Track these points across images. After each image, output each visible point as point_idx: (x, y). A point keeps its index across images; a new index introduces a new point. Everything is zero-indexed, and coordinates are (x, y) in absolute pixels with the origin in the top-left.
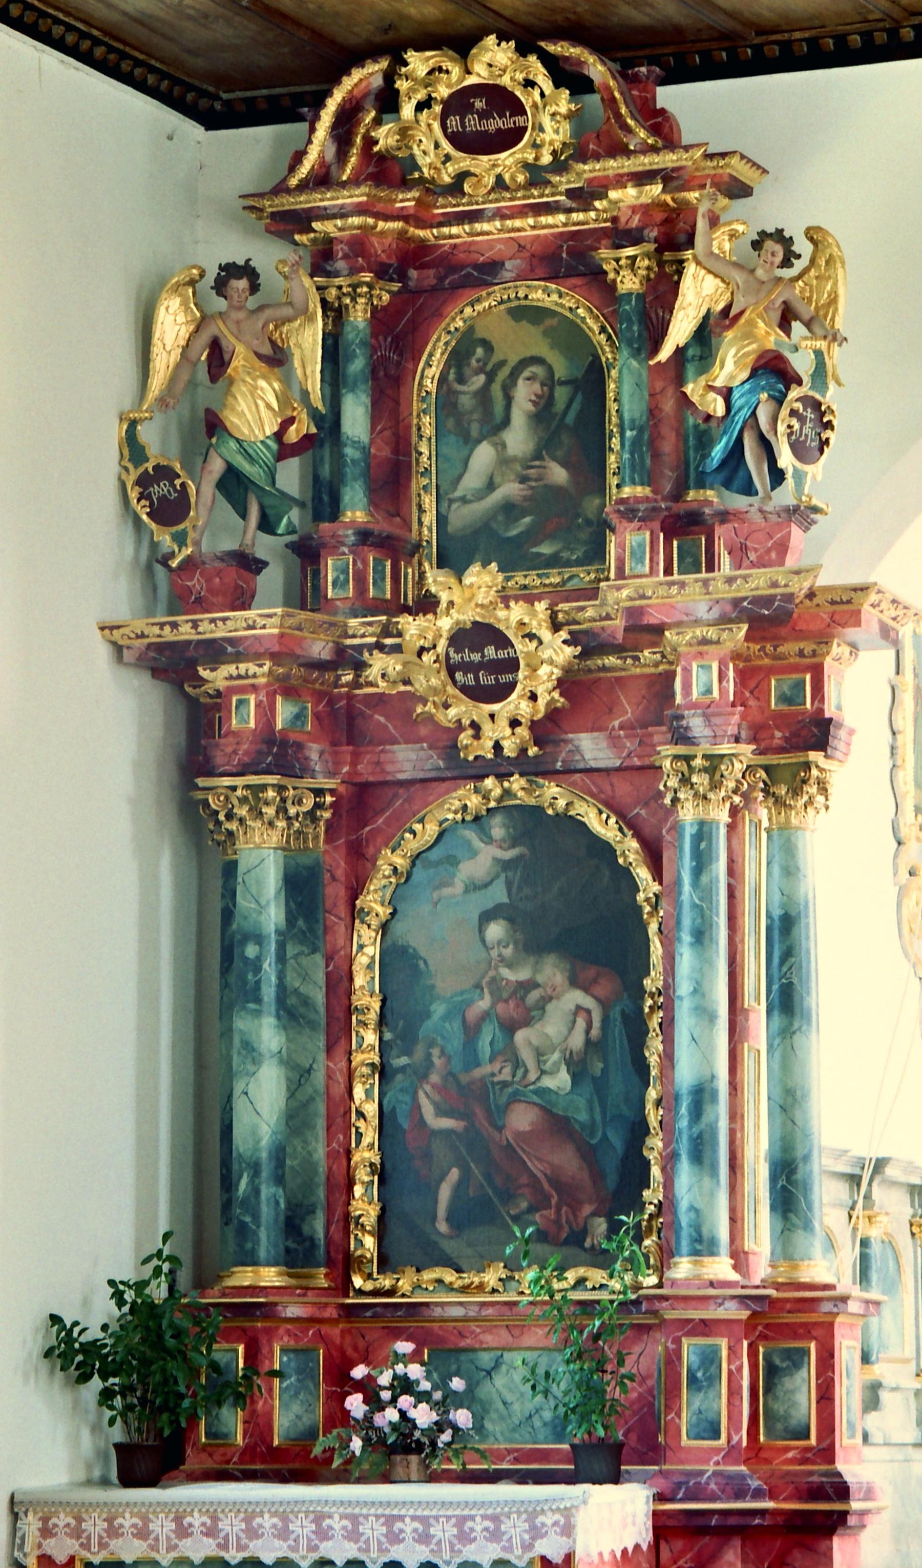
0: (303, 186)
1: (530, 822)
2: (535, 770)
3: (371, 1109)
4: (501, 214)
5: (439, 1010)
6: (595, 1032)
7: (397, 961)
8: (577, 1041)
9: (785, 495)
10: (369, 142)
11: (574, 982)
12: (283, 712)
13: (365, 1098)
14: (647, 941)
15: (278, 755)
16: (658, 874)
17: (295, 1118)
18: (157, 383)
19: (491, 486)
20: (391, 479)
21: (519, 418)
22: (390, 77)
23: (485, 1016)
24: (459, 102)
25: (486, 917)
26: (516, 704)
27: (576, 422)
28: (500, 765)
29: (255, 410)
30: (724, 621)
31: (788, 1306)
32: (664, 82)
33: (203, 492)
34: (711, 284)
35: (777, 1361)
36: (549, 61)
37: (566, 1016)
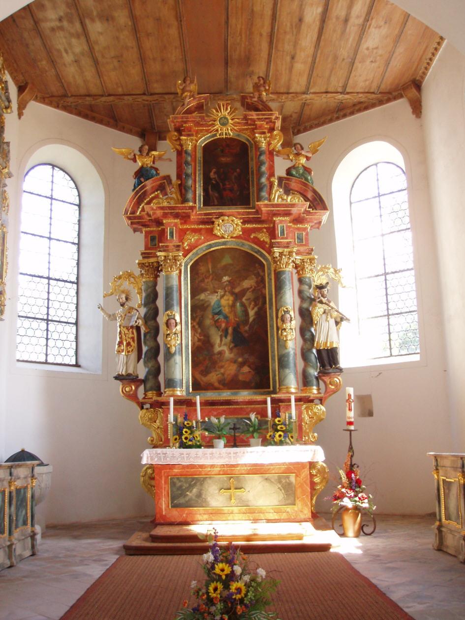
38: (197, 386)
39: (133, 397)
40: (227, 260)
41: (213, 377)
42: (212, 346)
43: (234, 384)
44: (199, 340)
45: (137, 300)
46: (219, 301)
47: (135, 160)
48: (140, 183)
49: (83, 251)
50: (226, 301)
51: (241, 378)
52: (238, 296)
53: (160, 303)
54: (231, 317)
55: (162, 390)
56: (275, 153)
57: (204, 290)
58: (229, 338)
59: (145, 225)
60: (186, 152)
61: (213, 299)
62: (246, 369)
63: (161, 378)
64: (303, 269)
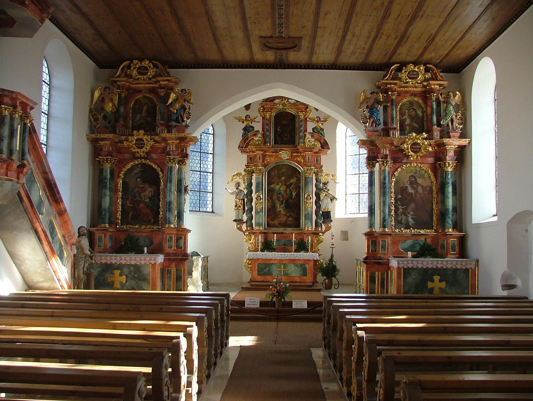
0: (117, 77)
1: (144, 165)
2: (145, 158)
3: (120, 203)
4: (143, 84)
5: (130, 190)
8: (150, 195)
9: (184, 124)
10: (126, 72)
12: (111, 149)
13: (120, 201)
14: (160, 182)
15: (110, 154)
16: (163, 173)
17: (111, 204)
18: (94, 103)
20: (126, 118)
21: (144, 111)
22: (130, 64)
24: (139, 68)
25: (137, 178)
26: (144, 149)
27: (152, 112)
28: (141, 158)
29: (109, 107)
30: (176, 140)
32: (168, 68)
33: (100, 117)
34: (174, 95)
36: (153, 64)
37: (149, 192)
38: (269, 225)
39: (240, 229)
40: (284, 170)
41: (276, 222)
42: (276, 208)
43: (285, 225)
44: (270, 205)
45: (242, 187)
46: (280, 188)
47: (243, 123)
48: (245, 134)
49: (215, 157)
50: (283, 188)
51: (288, 222)
52: (288, 186)
53: (254, 188)
54: (285, 195)
55: (254, 226)
56: (308, 119)
57: (274, 183)
58: (283, 205)
59: (247, 152)
60: (267, 119)
61: (277, 187)
62: (290, 219)
63: (253, 221)
64: (318, 175)
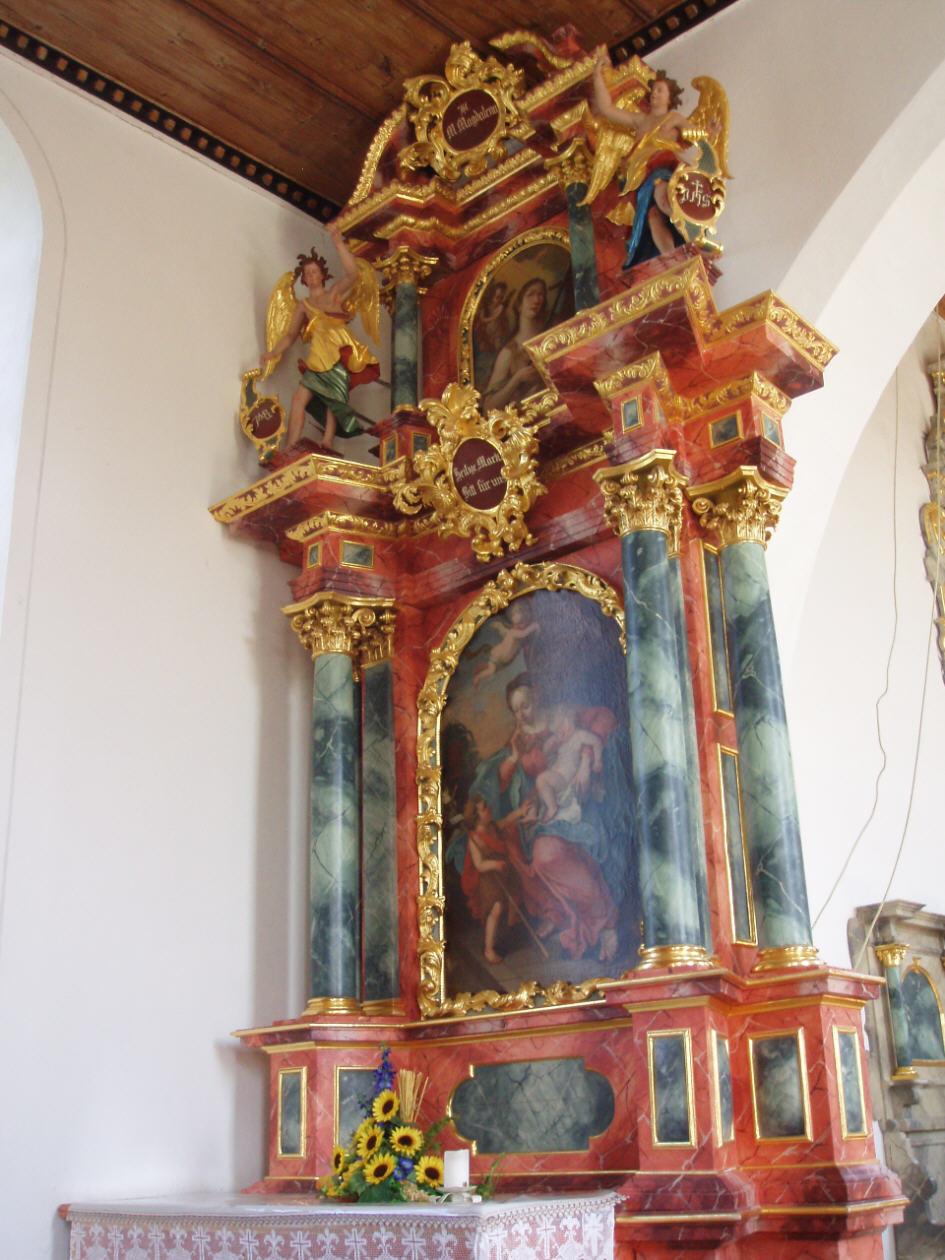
2: (537, 556)
5: (481, 770)
6: (598, 764)
7: (454, 740)
8: (584, 775)
11: (579, 724)
19: (509, 375)
23: (515, 768)
26: (512, 502)
31: (769, 992)
35: (766, 1052)
